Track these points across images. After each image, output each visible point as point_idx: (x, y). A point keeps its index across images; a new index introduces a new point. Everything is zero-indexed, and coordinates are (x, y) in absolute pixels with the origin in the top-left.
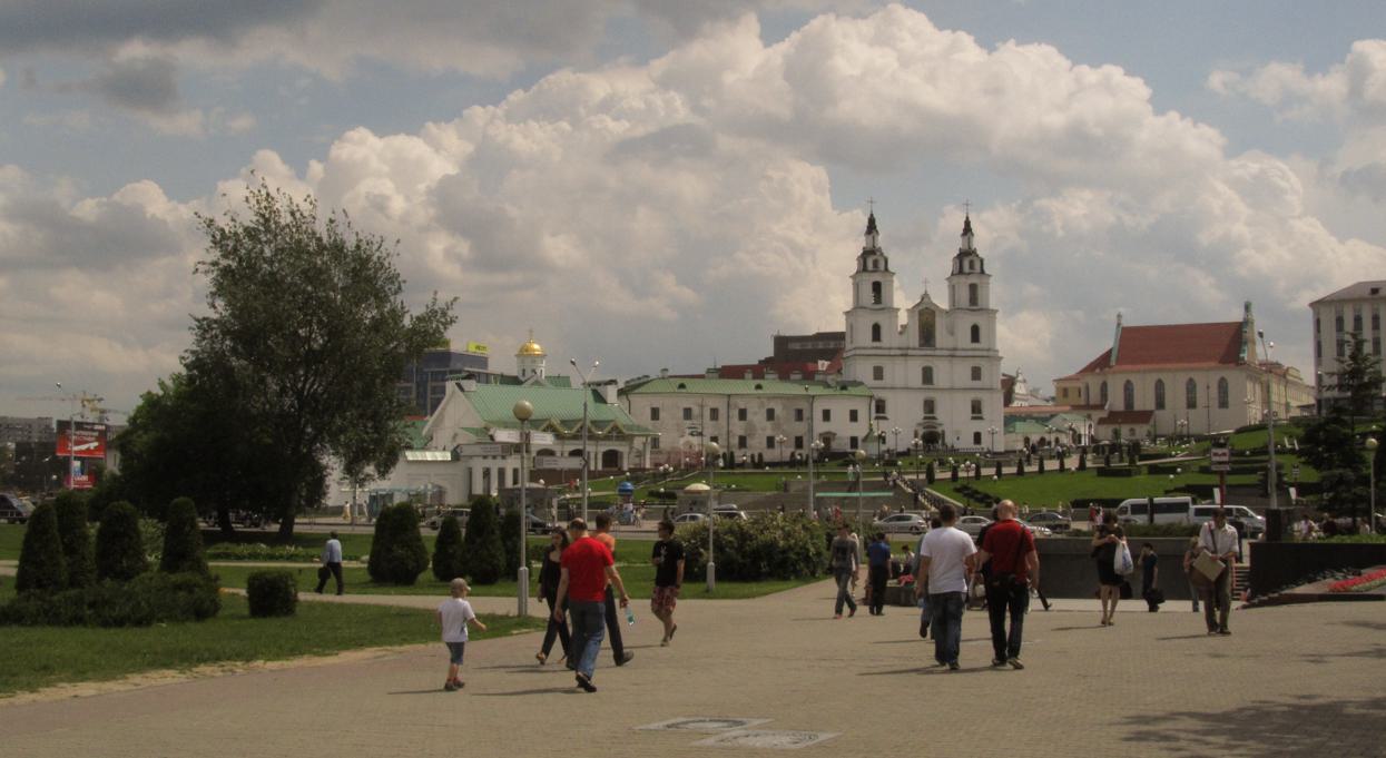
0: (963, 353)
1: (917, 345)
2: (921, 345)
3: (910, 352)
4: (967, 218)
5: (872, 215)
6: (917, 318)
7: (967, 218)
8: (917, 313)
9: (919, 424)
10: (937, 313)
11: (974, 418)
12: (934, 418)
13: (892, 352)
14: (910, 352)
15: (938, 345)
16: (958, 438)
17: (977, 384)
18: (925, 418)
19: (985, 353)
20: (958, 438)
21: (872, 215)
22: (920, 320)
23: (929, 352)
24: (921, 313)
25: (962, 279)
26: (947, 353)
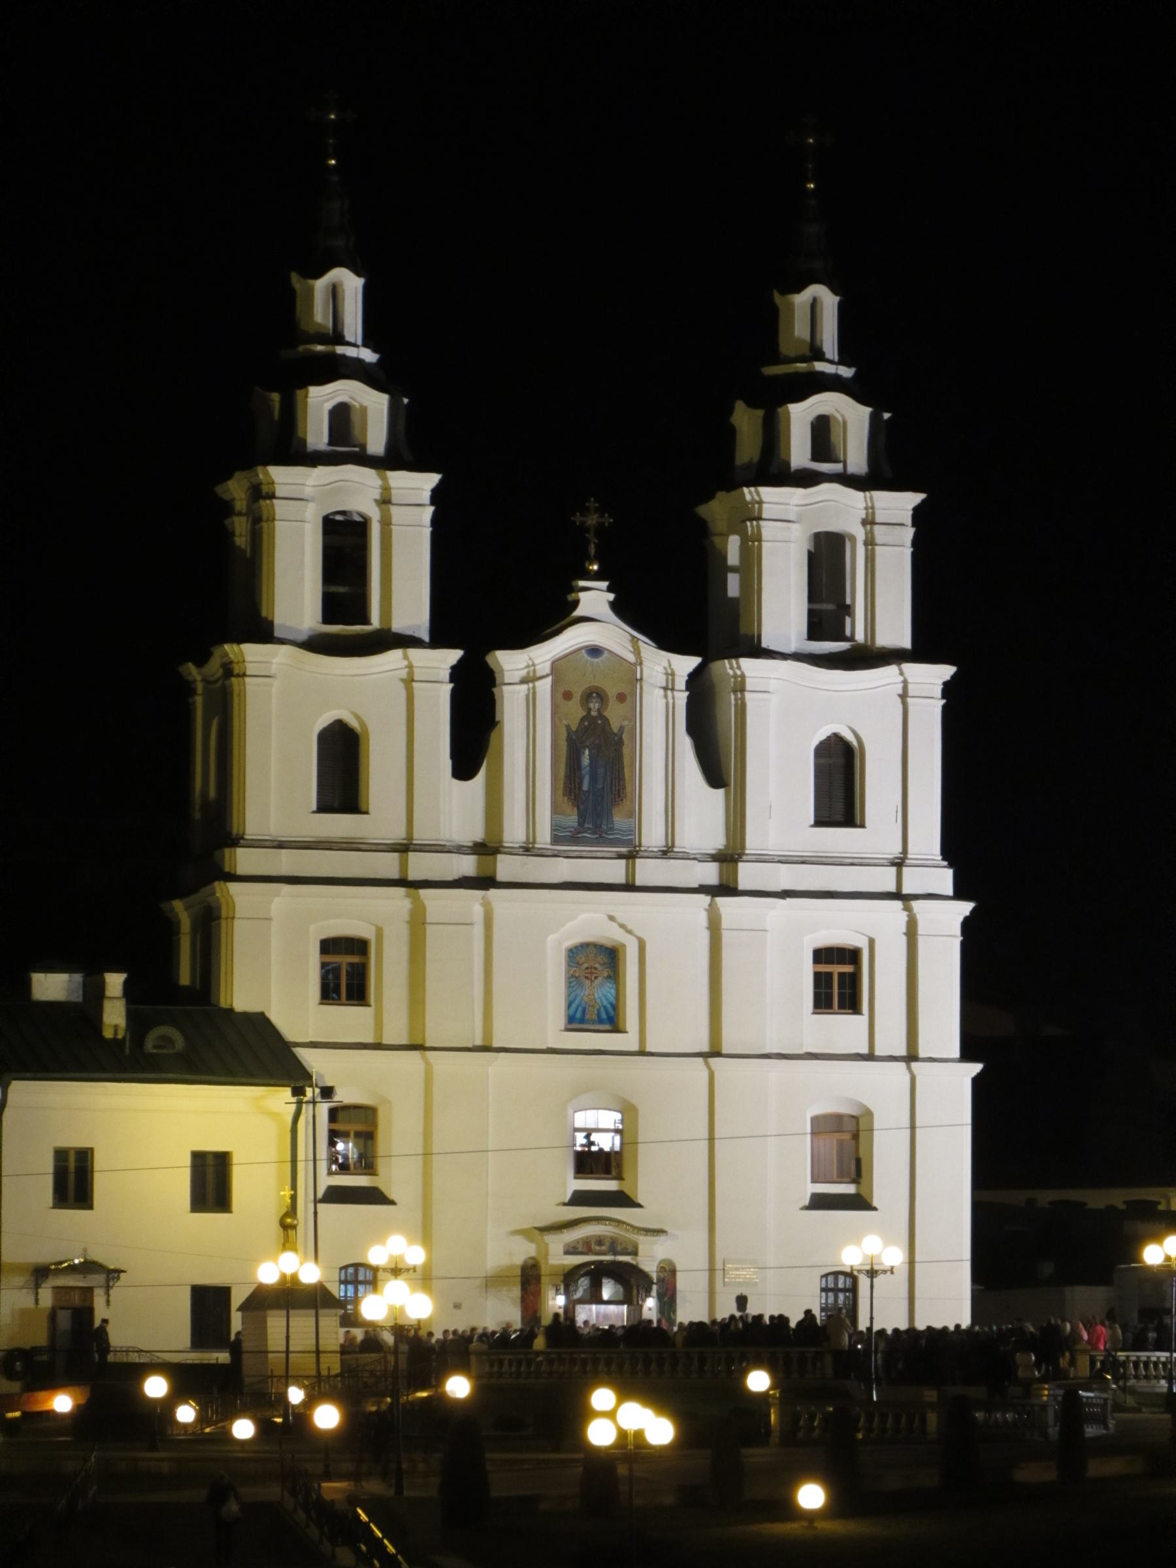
1: (544, 837)
13: (421, 866)
18: (579, 1198)
23: (614, 871)
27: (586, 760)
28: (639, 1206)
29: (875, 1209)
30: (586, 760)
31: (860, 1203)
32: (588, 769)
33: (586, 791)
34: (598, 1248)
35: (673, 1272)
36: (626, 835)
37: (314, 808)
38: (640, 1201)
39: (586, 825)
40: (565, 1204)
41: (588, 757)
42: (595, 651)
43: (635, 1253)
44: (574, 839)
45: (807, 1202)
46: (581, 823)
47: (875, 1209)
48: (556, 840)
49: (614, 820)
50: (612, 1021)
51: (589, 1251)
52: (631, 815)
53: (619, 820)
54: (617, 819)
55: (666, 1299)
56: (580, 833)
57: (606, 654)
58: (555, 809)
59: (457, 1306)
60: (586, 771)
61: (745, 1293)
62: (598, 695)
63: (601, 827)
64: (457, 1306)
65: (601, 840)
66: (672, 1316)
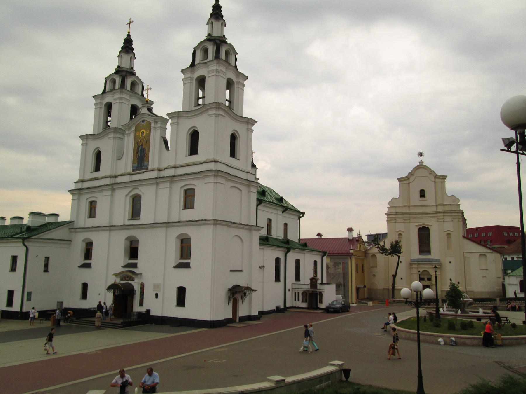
5: (129, 36)
6: (132, 136)
10: (153, 125)
11: (179, 266)
14: (120, 180)
15: (150, 167)
16: (157, 295)
17: (189, 215)
20: (157, 295)
21: (129, 36)
22: (136, 137)
30: (140, 149)
31: (187, 266)
34: (127, 279)
35: (144, 286)
39: (139, 166)
40: (122, 267)
41: (140, 148)
42: (143, 121)
44: (137, 170)
46: (138, 165)
48: (133, 171)
51: (125, 280)
52: (148, 161)
53: (145, 163)
56: (137, 168)
57: (146, 121)
59: (99, 294)
60: (140, 152)
62: (143, 132)
65: (142, 169)
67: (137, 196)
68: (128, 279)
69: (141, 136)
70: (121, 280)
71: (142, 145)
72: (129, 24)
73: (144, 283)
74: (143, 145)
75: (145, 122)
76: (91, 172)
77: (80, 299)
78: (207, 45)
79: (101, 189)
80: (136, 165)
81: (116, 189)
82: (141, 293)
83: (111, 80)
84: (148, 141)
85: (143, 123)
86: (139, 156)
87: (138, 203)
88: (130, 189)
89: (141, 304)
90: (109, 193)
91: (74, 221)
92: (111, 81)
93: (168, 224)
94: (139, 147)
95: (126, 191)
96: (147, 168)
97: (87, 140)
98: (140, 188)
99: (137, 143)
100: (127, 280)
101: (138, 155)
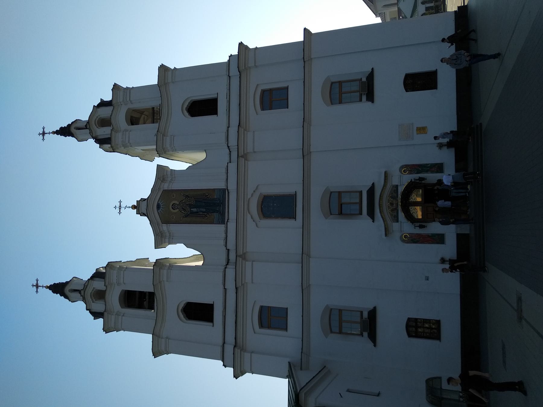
0: (233, 131)
2: (222, 220)
3: (231, 245)
4: (57, 132)
7: (57, 132)
8: (165, 227)
9: (387, 232)
10: (166, 186)
12: (371, 191)
14: (231, 245)
15: (222, 186)
18: (371, 214)
19: (235, 83)
24: (166, 221)
25: (118, 138)
26: (233, 167)
27: (195, 210)
28: (373, 184)
29: (373, 69)
30: (195, 210)
32: (198, 209)
33: (206, 210)
34: (394, 205)
35: (406, 166)
36: (221, 192)
37: (211, 324)
38: (371, 184)
39: (218, 209)
42: (158, 207)
43: (397, 186)
44: (223, 214)
45: (370, 103)
47: (373, 69)
49: (216, 198)
50: (291, 199)
51: (396, 209)
54: (215, 196)
55: (420, 169)
56: (220, 212)
57: (159, 202)
58: (212, 223)
59: (427, 278)
61: (415, 129)
63: (218, 203)
64: (427, 278)
66: (429, 165)
67: (262, 208)
68: (394, 202)
69: (178, 210)
70: (397, 221)
71: (191, 206)
72: (37, 286)
73: (402, 167)
74: (191, 203)
75: (160, 203)
76: (213, 326)
77: (440, 341)
78: (96, 117)
79: (239, 284)
80: (216, 215)
81: (245, 252)
82: (418, 173)
83: (92, 300)
84: (186, 194)
85: (160, 208)
86: (204, 210)
87: (272, 205)
88: (249, 216)
89: (439, 168)
90: (248, 264)
91: (289, 363)
92: (94, 300)
93: (306, 122)
94: (192, 213)
95: (250, 224)
96: (224, 190)
97: (162, 338)
98: (249, 196)
99: (186, 216)
100: (398, 206)
101: (203, 212)
